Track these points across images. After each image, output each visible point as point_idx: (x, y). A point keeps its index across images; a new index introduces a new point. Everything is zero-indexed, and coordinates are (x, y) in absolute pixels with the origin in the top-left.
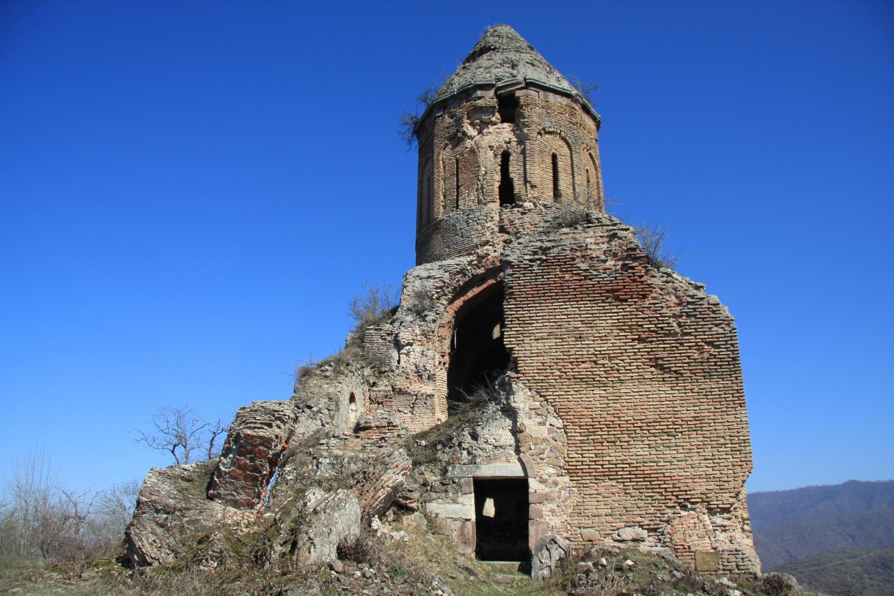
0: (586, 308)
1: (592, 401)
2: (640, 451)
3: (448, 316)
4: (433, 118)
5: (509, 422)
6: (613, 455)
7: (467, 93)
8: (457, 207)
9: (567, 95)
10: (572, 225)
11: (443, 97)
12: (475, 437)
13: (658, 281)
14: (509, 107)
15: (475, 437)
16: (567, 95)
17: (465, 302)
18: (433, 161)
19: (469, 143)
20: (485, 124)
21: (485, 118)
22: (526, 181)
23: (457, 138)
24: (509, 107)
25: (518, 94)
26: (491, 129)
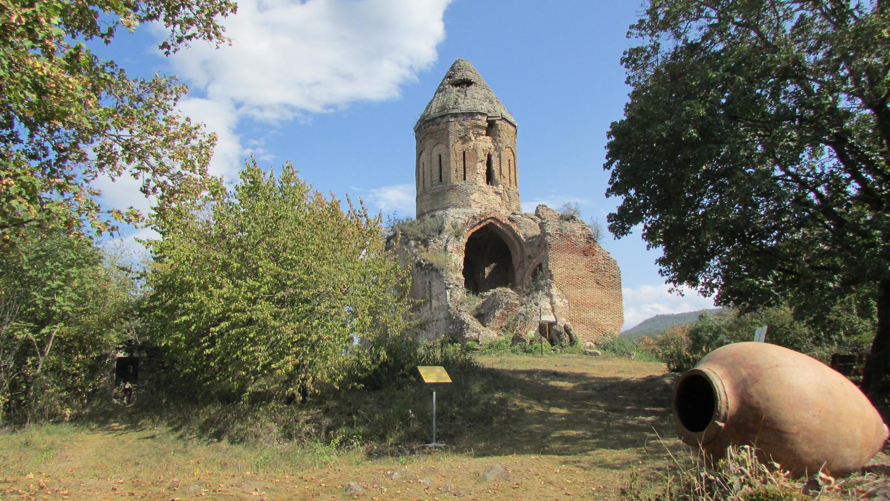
0: (575, 256)
1: (576, 293)
2: (592, 314)
3: (466, 240)
4: (445, 120)
5: (549, 299)
6: (584, 315)
7: (471, 114)
8: (465, 179)
9: (514, 126)
10: (568, 220)
11: (456, 111)
12: (536, 304)
13: (597, 249)
14: (491, 128)
15: (536, 304)
16: (514, 126)
17: (473, 233)
18: (447, 146)
19: (471, 144)
20: (480, 134)
21: (480, 131)
22: (501, 174)
23: (465, 139)
24: (491, 128)
25: (497, 122)
26: (482, 137)
